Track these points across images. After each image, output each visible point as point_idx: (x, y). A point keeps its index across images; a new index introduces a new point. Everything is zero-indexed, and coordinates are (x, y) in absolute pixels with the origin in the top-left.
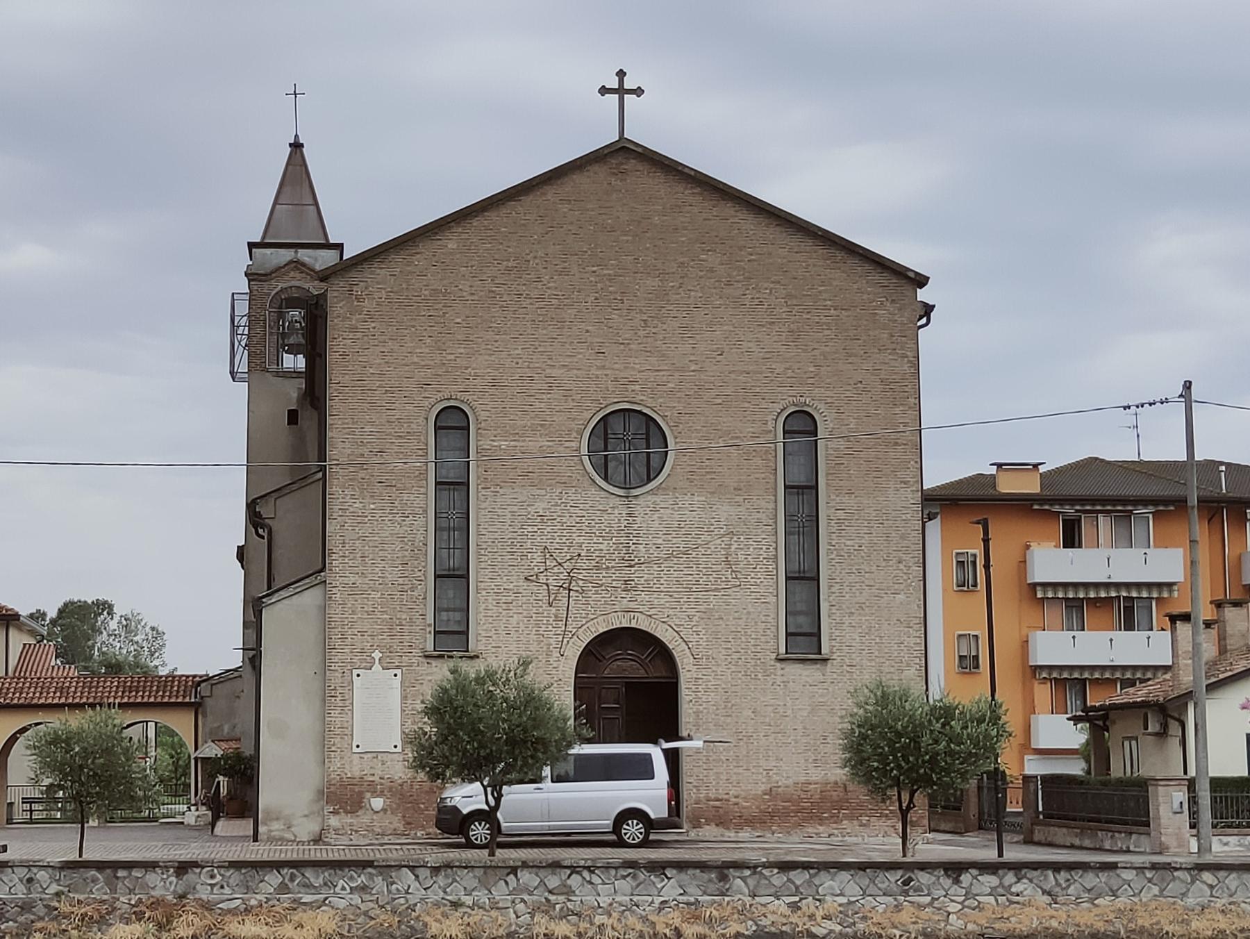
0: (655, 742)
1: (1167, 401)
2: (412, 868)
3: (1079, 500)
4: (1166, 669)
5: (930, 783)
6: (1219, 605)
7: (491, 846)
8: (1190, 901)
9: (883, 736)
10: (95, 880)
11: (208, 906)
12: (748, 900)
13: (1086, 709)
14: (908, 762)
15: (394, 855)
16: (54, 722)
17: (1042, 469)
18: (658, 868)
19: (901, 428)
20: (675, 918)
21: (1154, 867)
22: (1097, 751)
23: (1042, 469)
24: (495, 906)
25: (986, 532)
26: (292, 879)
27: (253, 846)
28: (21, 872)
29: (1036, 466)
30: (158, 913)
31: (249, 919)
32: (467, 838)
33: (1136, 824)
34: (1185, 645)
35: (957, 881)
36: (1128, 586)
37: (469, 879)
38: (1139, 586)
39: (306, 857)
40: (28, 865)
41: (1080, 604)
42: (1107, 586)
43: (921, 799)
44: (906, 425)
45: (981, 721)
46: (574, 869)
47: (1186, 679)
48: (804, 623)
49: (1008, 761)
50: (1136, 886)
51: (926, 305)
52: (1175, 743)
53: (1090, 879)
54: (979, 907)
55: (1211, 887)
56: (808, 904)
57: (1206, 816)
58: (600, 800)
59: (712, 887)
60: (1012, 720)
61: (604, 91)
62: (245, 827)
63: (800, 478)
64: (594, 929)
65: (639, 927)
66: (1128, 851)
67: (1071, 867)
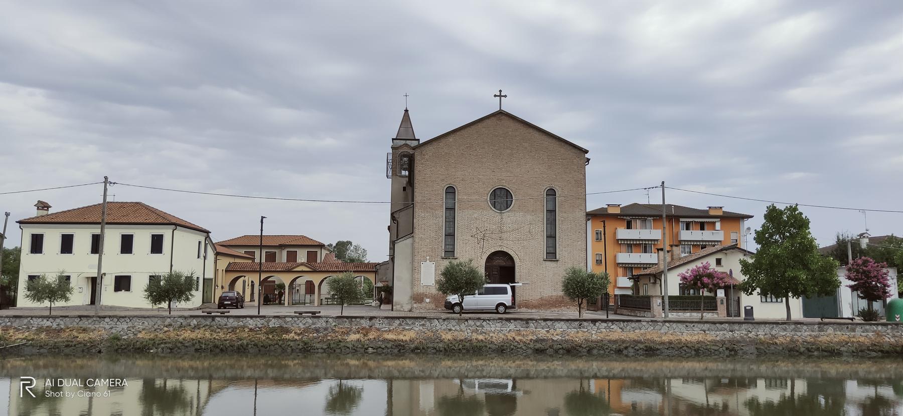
3: (631, 215)
6: (671, 246)
8: (662, 331)
11: (378, 330)
15: (432, 315)
18: (508, 320)
20: (513, 334)
21: (652, 321)
22: (636, 288)
24: (461, 331)
28: (325, 319)
34: (661, 257)
37: (454, 322)
41: (632, 245)
43: (585, 301)
46: (484, 320)
47: (662, 267)
48: (551, 250)
49: (610, 290)
52: (658, 285)
53: (633, 325)
54: (601, 332)
57: (667, 307)
58: (492, 300)
60: (611, 278)
61: (495, 96)
62: (389, 307)
63: (551, 208)
67: (628, 321)
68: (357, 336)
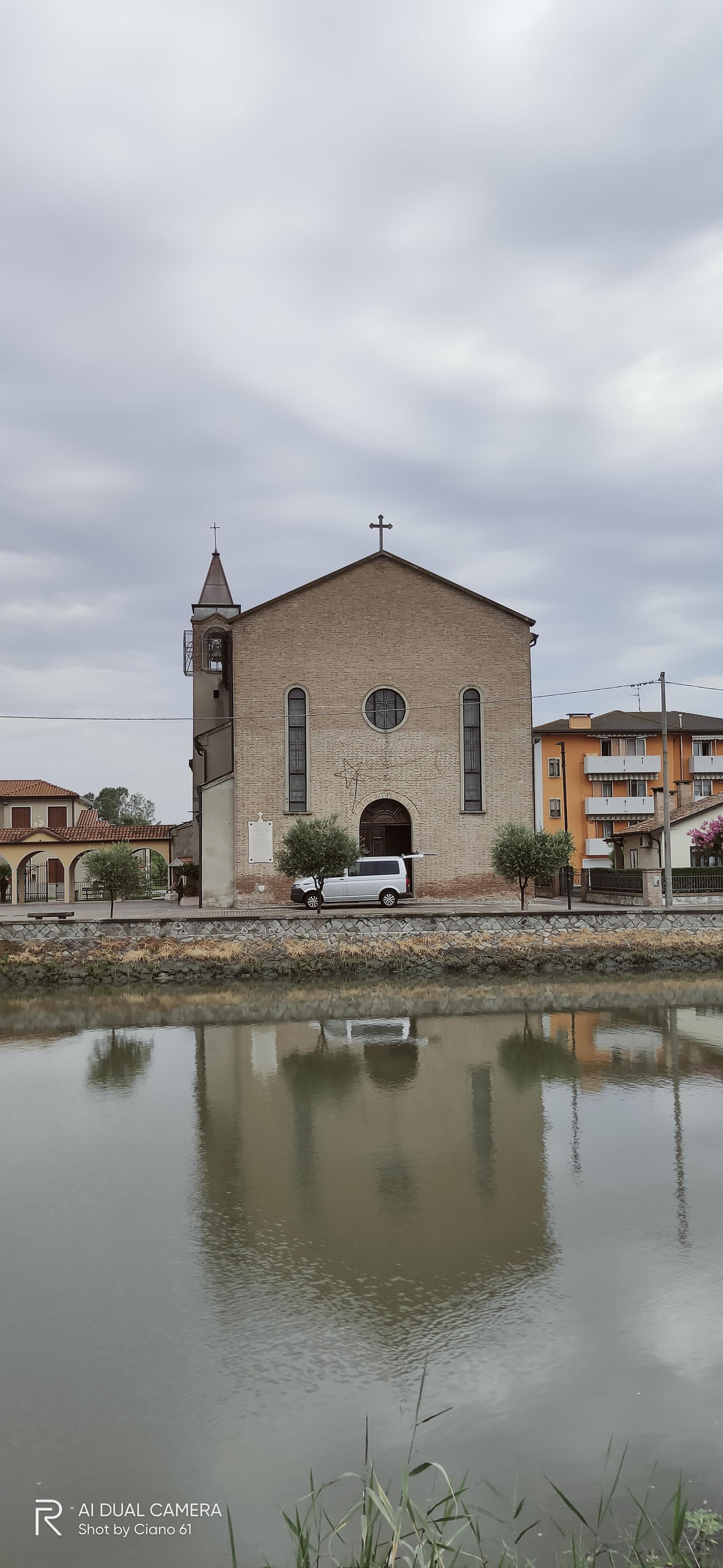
0: (400, 856)
1: (653, 682)
2: (279, 920)
3: (609, 732)
4: (652, 815)
5: (535, 873)
6: (677, 783)
7: (319, 908)
8: (662, 929)
9: (512, 851)
10: (119, 929)
11: (176, 941)
12: (445, 932)
13: (612, 836)
14: (524, 863)
15: (270, 914)
16: (97, 850)
17: (592, 717)
18: (401, 917)
19: (522, 697)
20: (409, 942)
21: (644, 913)
22: (618, 856)
23: (592, 717)
24: (320, 938)
25: (563, 749)
26: (219, 927)
27: (199, 911)
28: (82, 926)
29: (589, 715)
30: (151, 945)
31: (197, 947)
32: (307, 904)
33: (636, 892)
34: (661, 803)
35: (548, 922)
36: (634, 774)
37: (307, 925)
38: (639, 774)
39: (226, 916)
40: (85, 922)
41: (611, 784)
42: (623, 774)
43: (531, 882)
44: (524, 695)
45: (560, 843)
46: (359, 919)
47: (661, 820)
48: (473, 795)
49: (574, 861)
50: (636, 922)
51: (534, 635)
52: (655, 852)
53: (614, 920)
54: (559, 934)
55: (672, 922)
56: (475, 934)
57: (670, 887)
58: (371, 885)
59: (428, 927)
60: (576, 842)
61: (372, 526)
62: (195, 901)
63: (471, 722)
64: (370, 948)
65: (392, 947)
66: (632, 905)
67: (604, 913)
68: (140, 954)
